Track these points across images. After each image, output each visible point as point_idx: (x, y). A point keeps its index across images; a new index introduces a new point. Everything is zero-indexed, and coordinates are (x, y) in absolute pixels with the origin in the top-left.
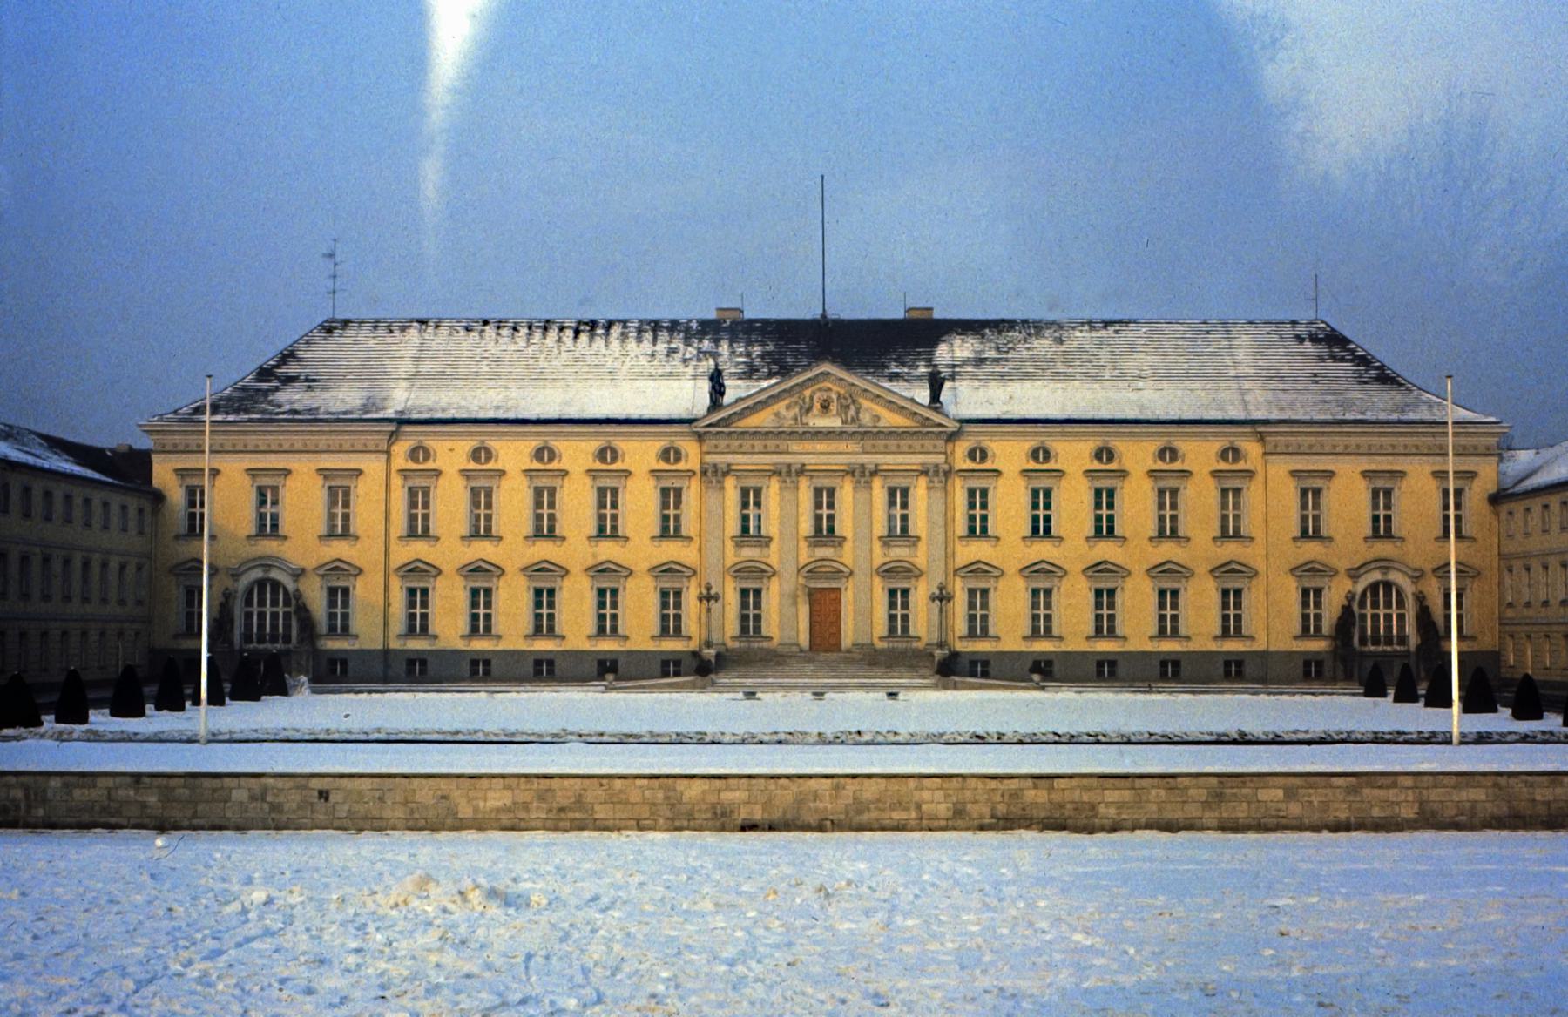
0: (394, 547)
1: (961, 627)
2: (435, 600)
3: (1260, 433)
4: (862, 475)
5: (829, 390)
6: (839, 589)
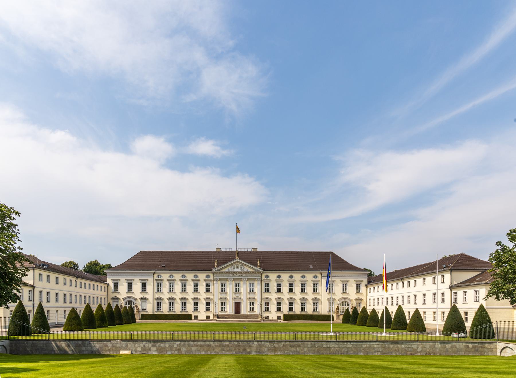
1: (264, 309)
4: (245, 281)
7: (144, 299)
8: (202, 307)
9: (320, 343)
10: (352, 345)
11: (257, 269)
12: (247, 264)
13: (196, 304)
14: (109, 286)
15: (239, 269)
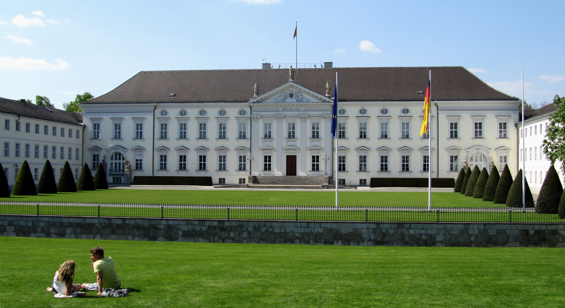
0: (156, 141)
2: (168, 159)
3: (436, 104)
5: (293, 90)
6: (296, 156)
7: (139, 149)
8: (232, 162)
9: (268, 224)
10: (323, 229)
11: (324, 98)
12: (308, 91)
13: (222, 159)
14: (86, 128)
15: (295, 97)
